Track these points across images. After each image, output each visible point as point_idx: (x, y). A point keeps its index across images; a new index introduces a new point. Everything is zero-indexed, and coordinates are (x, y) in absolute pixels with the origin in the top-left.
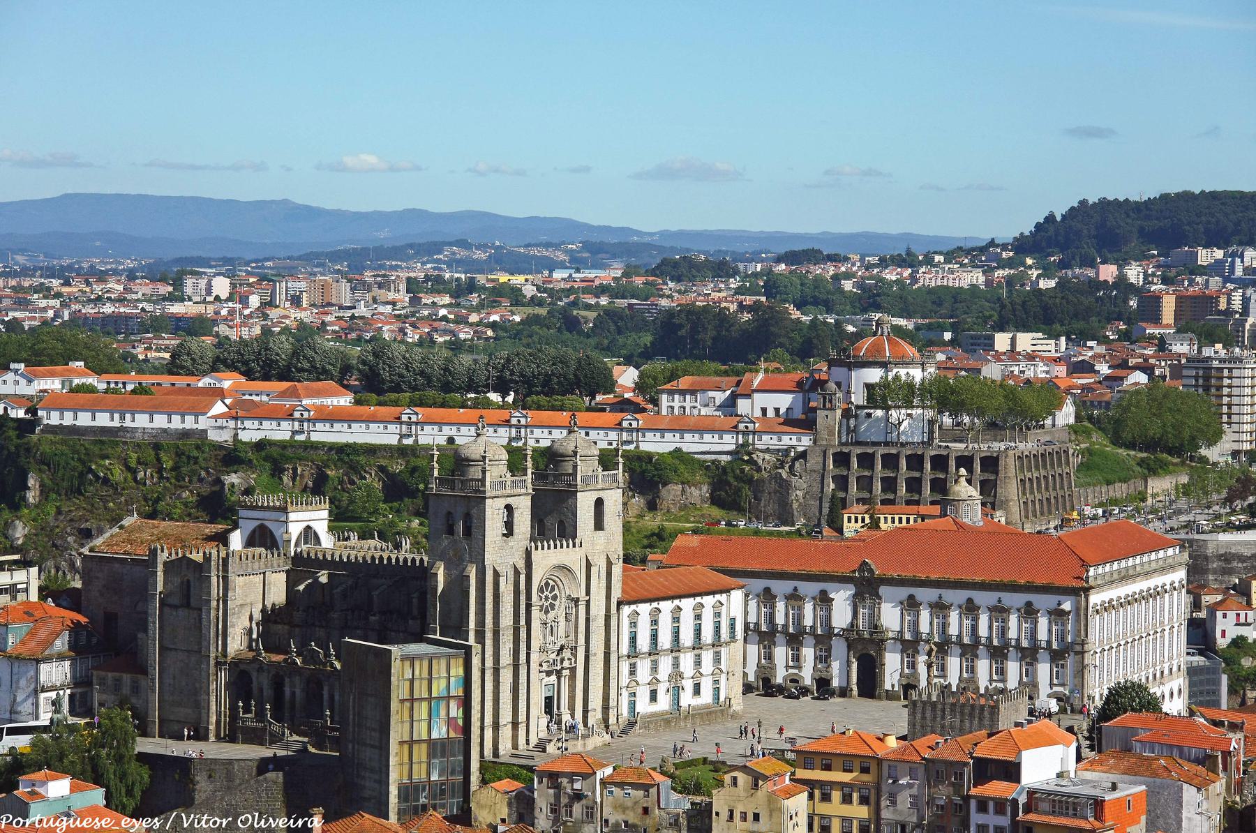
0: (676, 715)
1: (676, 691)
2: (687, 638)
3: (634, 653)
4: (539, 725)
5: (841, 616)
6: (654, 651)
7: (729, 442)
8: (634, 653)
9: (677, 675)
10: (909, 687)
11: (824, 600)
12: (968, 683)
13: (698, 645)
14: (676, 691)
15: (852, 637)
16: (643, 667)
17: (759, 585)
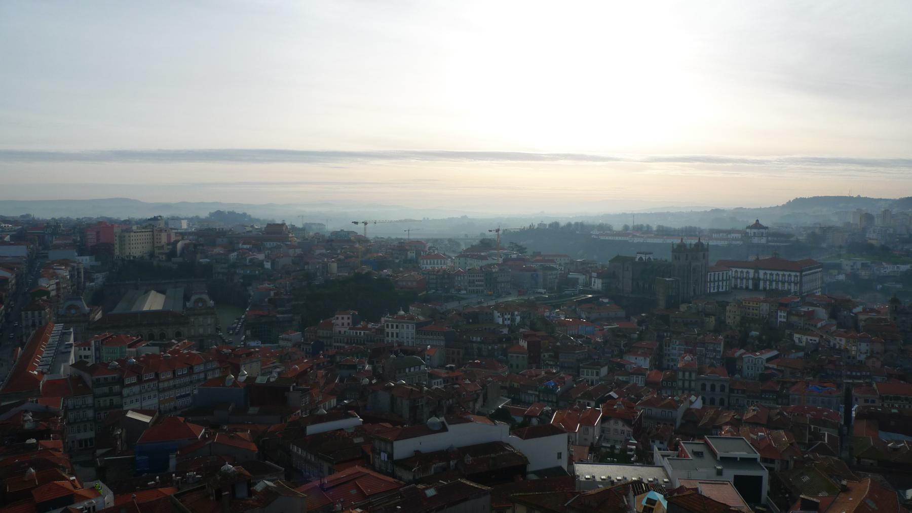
0: (718, 293)
1: (718, 288)
2: (721, 278)
3: (710, 281)
4: (692, 294)
5: (751, 275)
6: (714, 281)
7: (726, 243)
8: (710, 281)
9: (718, 286)
10: (765, 289)
11: (747, 272)
12: (777, 289)
13: (723, 280)
14: (718, 288)
15: (753, 279)
16: (712, 285)
17: (734, 270)
